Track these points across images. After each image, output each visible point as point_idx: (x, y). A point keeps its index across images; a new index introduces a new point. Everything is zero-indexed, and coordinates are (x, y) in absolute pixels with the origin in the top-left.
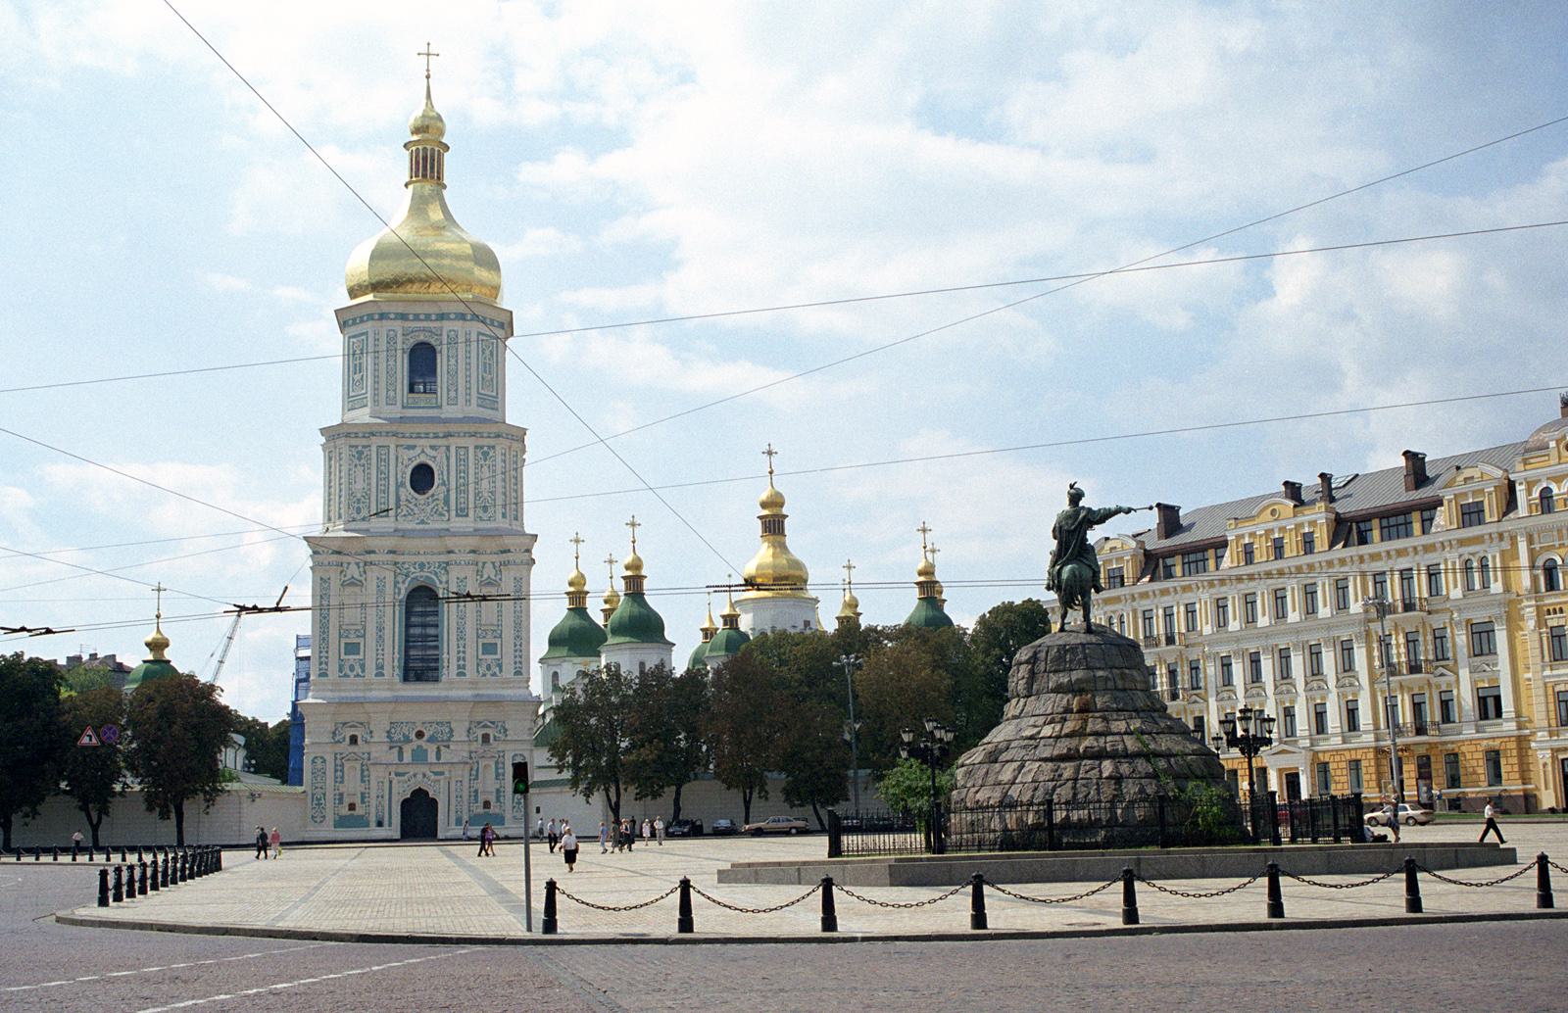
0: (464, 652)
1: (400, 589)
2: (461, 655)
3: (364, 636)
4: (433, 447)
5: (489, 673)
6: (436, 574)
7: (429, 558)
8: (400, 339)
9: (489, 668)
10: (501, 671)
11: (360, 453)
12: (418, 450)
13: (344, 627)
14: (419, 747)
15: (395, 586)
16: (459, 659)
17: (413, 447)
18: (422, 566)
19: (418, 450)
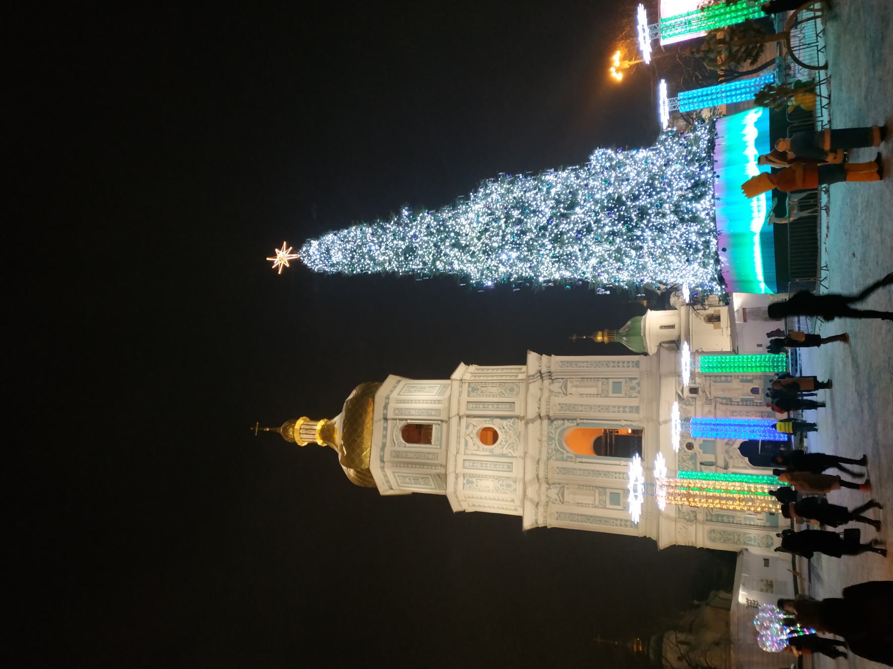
0: (619, 407)
1: (568, 457)
2: (621, 409)
3: (605, 488)
4: (467, 427)
5: (638, 388)
6: (557, 428)
7: (545, 433)
8: (397, 448)
9: (633, 388)
10: (635, 379)
11: (469, 482)
12: (468, 439)
13: (597, 503)
14: (701, 446)
15: (566, 460)
16: (624, 412)
17: (466, 442)
18: (550, 439)
19: (468, 439)
